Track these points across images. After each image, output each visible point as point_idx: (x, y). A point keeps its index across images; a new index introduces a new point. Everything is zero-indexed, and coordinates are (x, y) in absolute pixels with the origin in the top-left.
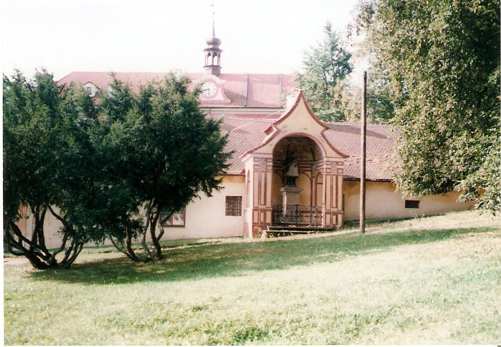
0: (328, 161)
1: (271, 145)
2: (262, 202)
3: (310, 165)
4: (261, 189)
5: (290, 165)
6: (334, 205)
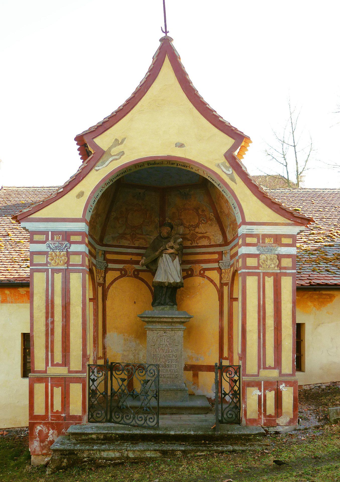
0: (251, 236)
1: (81, 194)
2: (58, 358)
3: (216, 256)
4: (53, 323)
5: (160, 255)
6: (270, 360)
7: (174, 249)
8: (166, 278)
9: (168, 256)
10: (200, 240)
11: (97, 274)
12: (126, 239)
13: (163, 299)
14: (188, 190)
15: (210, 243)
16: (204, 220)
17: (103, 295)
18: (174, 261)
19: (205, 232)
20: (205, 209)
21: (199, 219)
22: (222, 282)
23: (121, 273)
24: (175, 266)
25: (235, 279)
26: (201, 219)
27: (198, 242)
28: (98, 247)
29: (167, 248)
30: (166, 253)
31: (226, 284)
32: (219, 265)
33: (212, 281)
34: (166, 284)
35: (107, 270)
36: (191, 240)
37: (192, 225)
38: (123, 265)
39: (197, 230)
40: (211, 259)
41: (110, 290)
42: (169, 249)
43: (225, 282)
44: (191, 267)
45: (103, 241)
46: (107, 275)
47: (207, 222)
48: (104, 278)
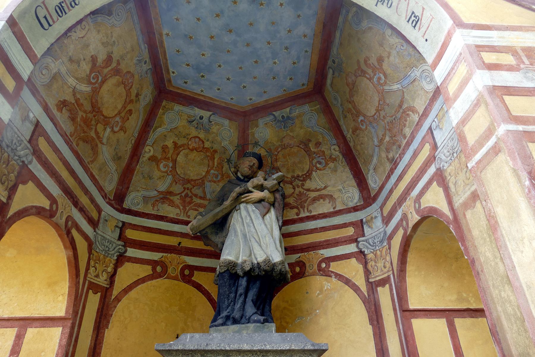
3: (350, 231)
5: (234, 207)
7: (266, 191)
8: (248, 253)
9: (251, 207)
10: (315, 205)
11: (92, 263)
12: (172, 204)
13: (238, 306)
14: (288, 110)
15: (334, 208)
16: (320, 163)
17: (101, 315)
18: (265, 218)
19: (323, 186)
20: (321, 140)
21: (311, 162)
22: (370, 280)
23: (154, 269)
24: (269, 226)
25: (408, 259)
26: (315, 161)
27: (310, 208)
28: (108, 210)
29: (250, 189)
30: (247, 202)
31: (383, 282)
32: (357, 246)
33: (347, 282)
34: (247, 268)
35: (121, 259)
36: (297, 208)
37: (298, 176)
38: (161, 254)
39: (309, 184)
40: (339, 238)
41: (120, 305)
42: (253, 190)
43: (378, 279)
44: (301, 259)
45: (122, 202)
46: (119, 270)
47: (327, 164)
48: (112, 277)
